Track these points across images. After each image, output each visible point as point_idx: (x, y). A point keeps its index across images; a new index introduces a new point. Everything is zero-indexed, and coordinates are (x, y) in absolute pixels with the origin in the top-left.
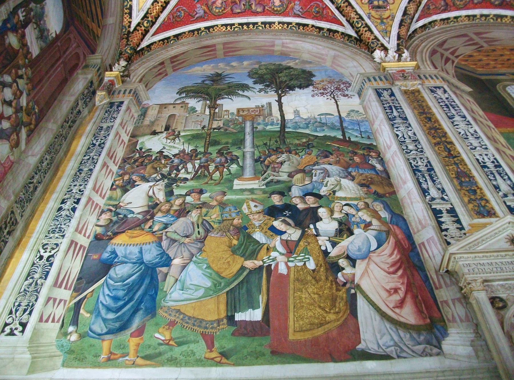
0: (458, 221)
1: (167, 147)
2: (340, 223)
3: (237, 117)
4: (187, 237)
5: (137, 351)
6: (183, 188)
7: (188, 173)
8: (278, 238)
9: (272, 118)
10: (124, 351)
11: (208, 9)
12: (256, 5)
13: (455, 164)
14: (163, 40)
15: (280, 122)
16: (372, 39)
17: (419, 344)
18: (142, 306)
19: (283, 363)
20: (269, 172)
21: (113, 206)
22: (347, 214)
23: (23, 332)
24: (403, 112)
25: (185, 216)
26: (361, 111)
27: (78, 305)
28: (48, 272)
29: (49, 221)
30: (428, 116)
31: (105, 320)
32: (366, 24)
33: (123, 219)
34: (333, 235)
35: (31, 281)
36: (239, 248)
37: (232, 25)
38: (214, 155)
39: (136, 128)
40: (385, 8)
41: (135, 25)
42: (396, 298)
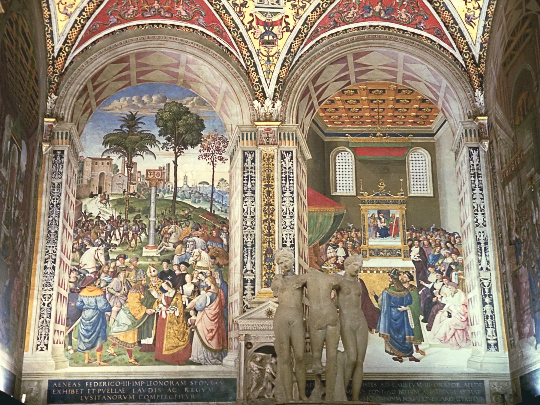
0: (254, 289)
1: (102, 213)
2: (195, 286)
3: (146, 181)
4: (119, 292)
5: (100, 358)
6: (115, 253)
7: (117, 240)
8: (163, 295)
9: (169, 184)
10: (95, 358)
11: (121, 17)
12: (164, 12)
13: (269, 242)
14: (82, 51)
15: (173, 190)
16: (257, 82)
17: (214, 359)
18: (100, 335)
19: (159, 365)
20: (163, 242)
21: (76, 266)
22: (200, 280)
23: (47, 349)
24: (255, 184)
25: (117, 277)
26: (228, 181)
27: (70, 334)
28: (50, 314)
29: (41, 277)
30: (270, 189)
31: (84, 342)
32: (254, 63)
33: (83, 277)
34: (190, 294)
35: (42, 319)
36: (144, 301)
37: (143, 25)
38: (132, 223)
39: (79, 188)
40: (273, 44)
41: (58, 51)
42: (211, 335)
